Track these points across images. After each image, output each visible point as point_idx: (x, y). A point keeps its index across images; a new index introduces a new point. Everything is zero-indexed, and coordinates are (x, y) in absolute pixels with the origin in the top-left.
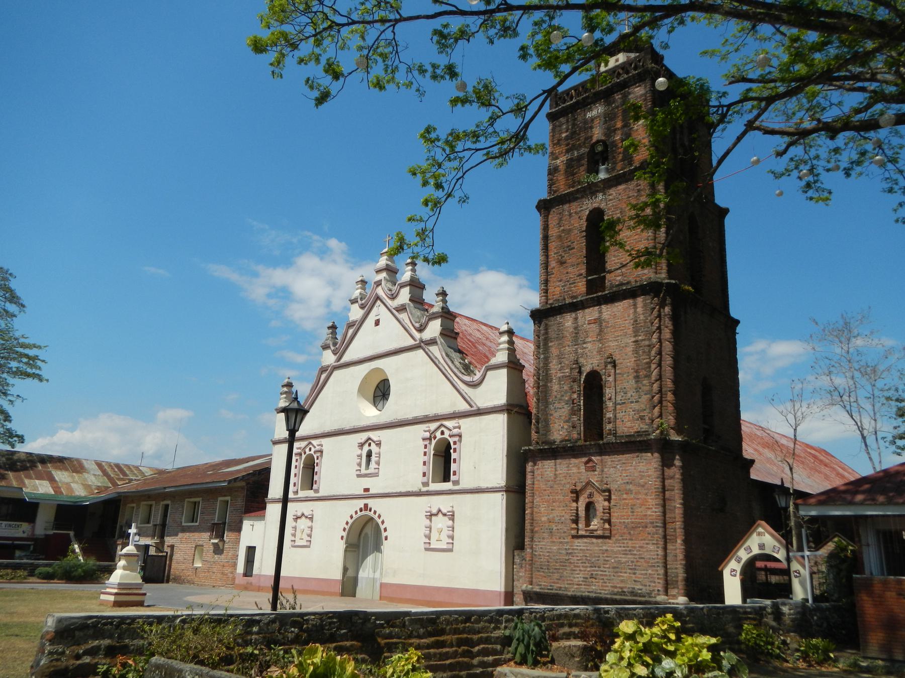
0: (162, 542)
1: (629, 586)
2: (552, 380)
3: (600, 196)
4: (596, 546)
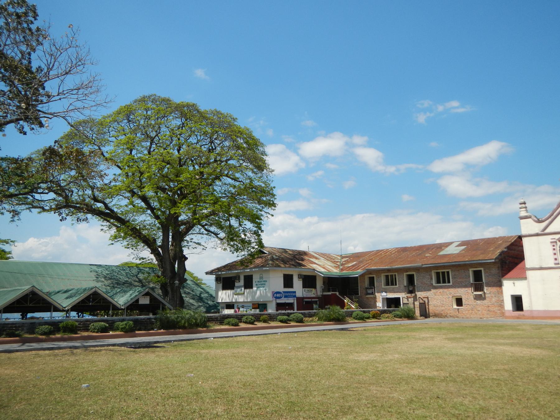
0: (416, 295)
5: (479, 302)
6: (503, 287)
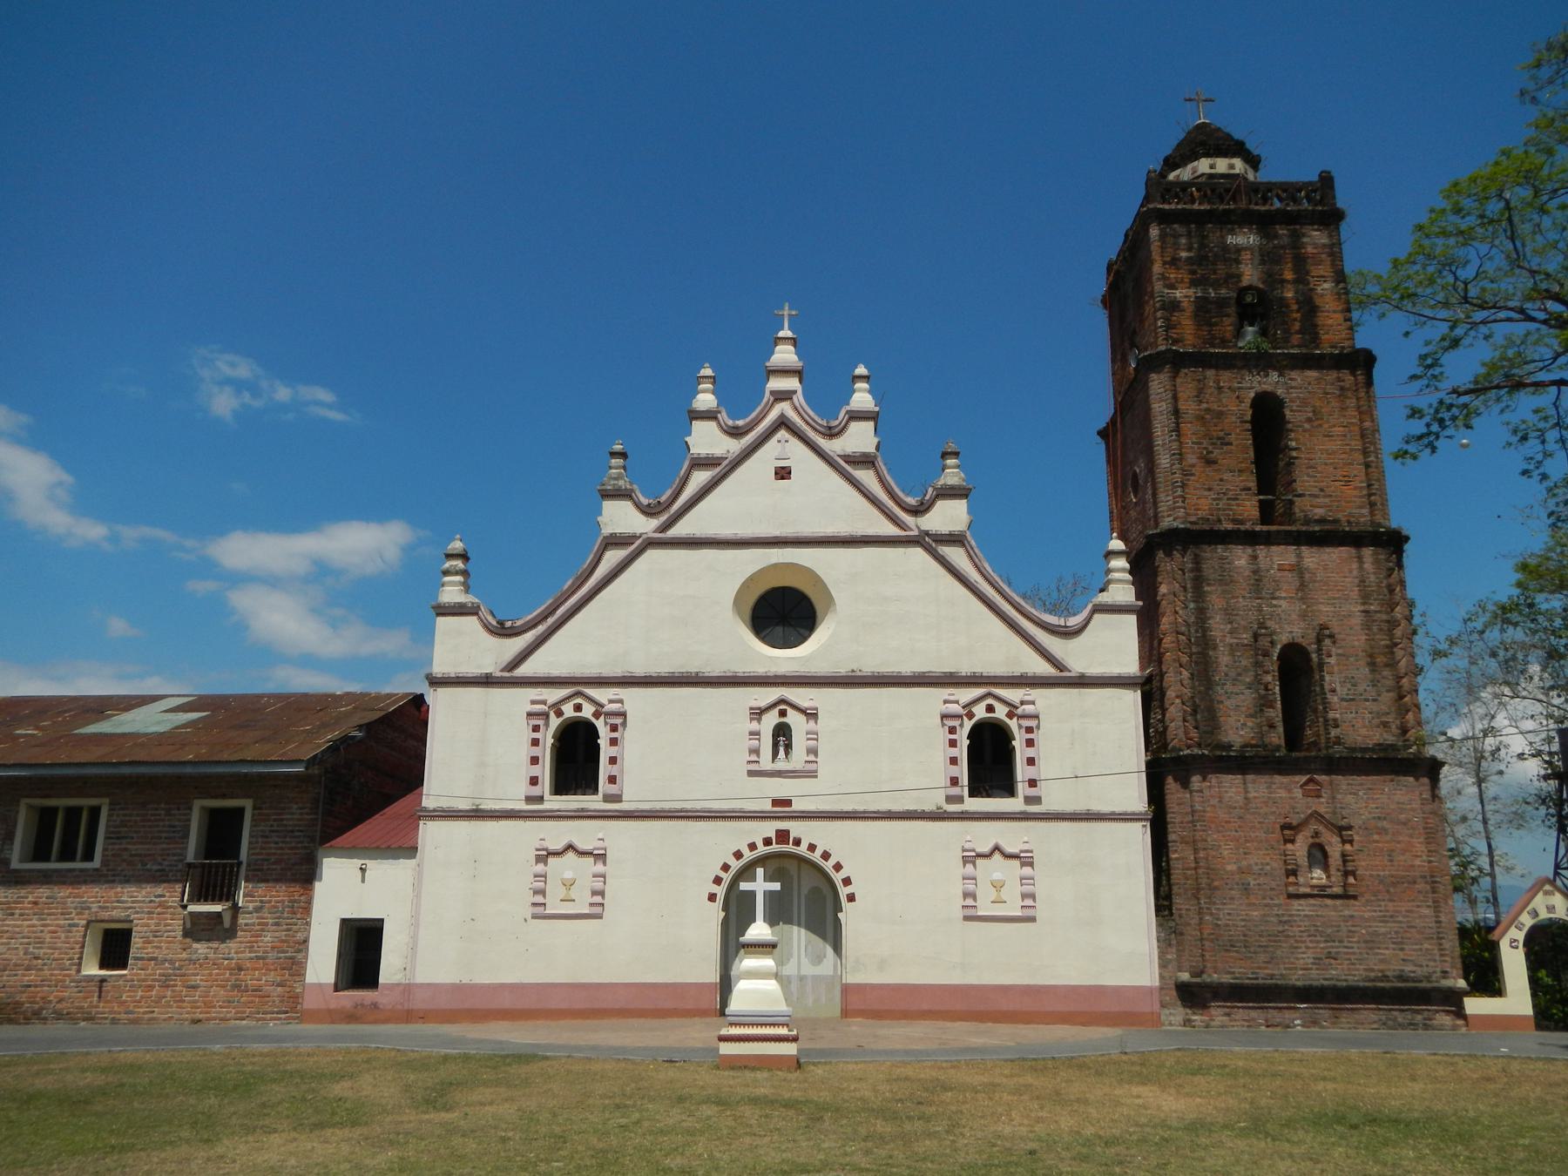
1: (1393, 968)
2: (1215, 648)
3: (1274, 376)
4: (1332, 911)
5: (201, 948)
6: (318, 885)
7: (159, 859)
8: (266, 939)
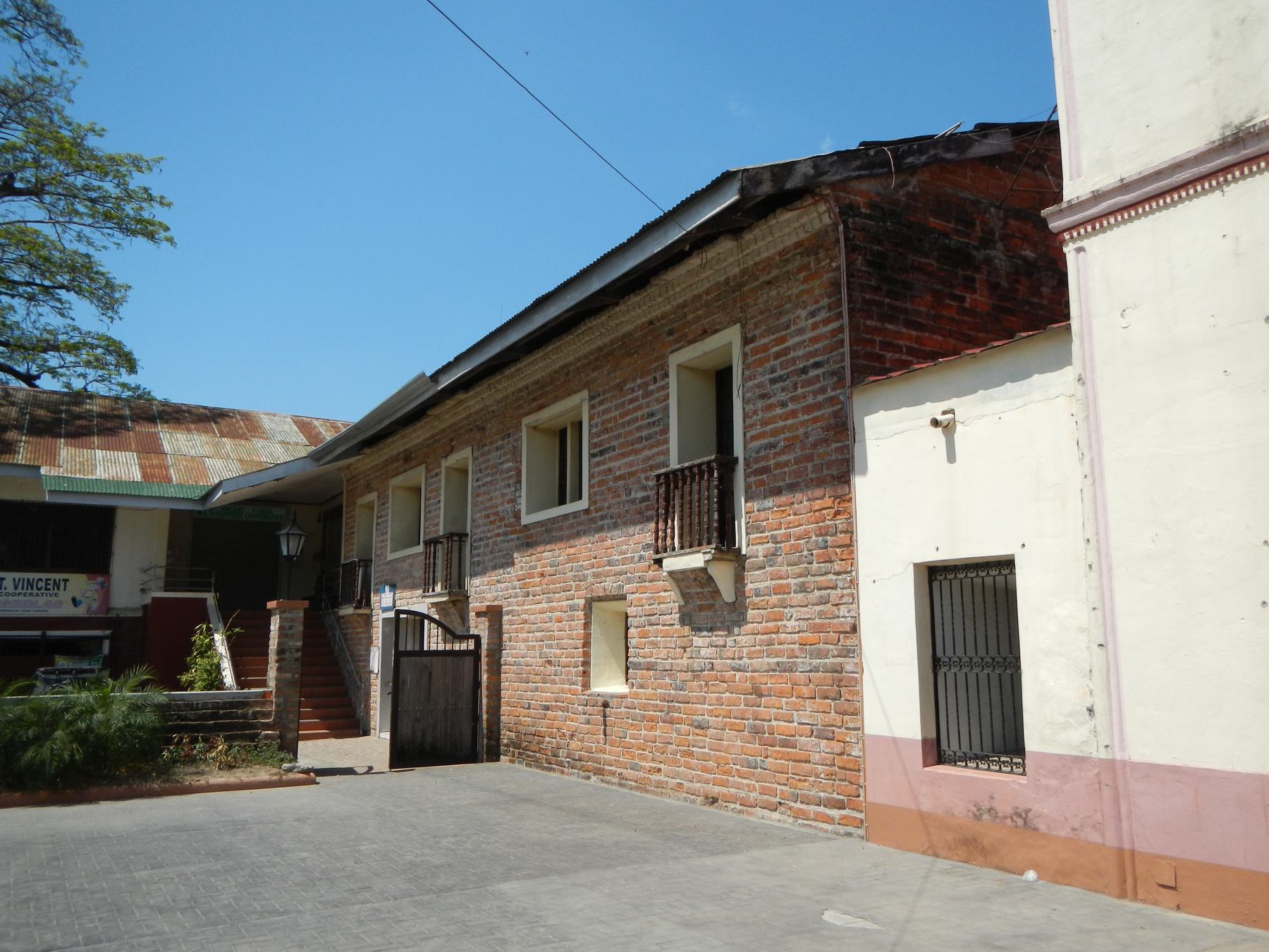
0: (458, 599)
6: (860, 484)
7: (643, 476)
8: (791, 624)
